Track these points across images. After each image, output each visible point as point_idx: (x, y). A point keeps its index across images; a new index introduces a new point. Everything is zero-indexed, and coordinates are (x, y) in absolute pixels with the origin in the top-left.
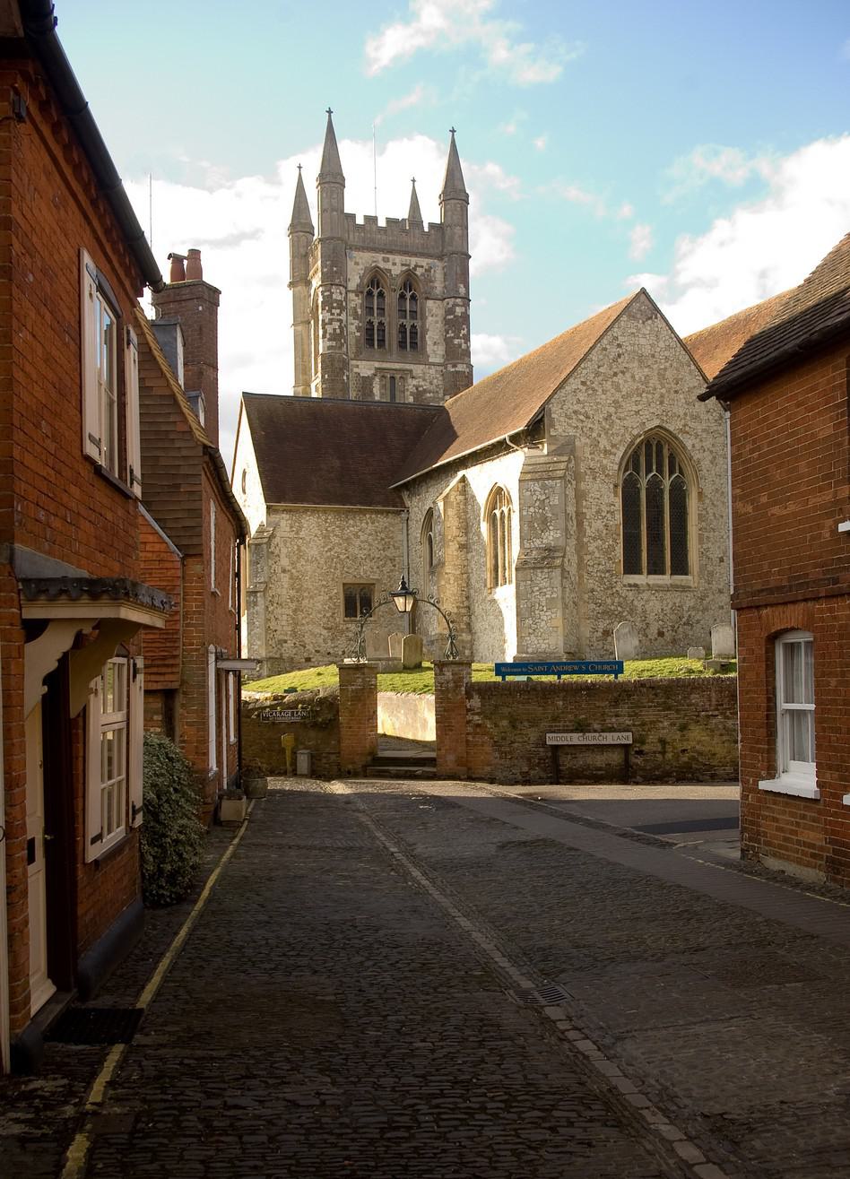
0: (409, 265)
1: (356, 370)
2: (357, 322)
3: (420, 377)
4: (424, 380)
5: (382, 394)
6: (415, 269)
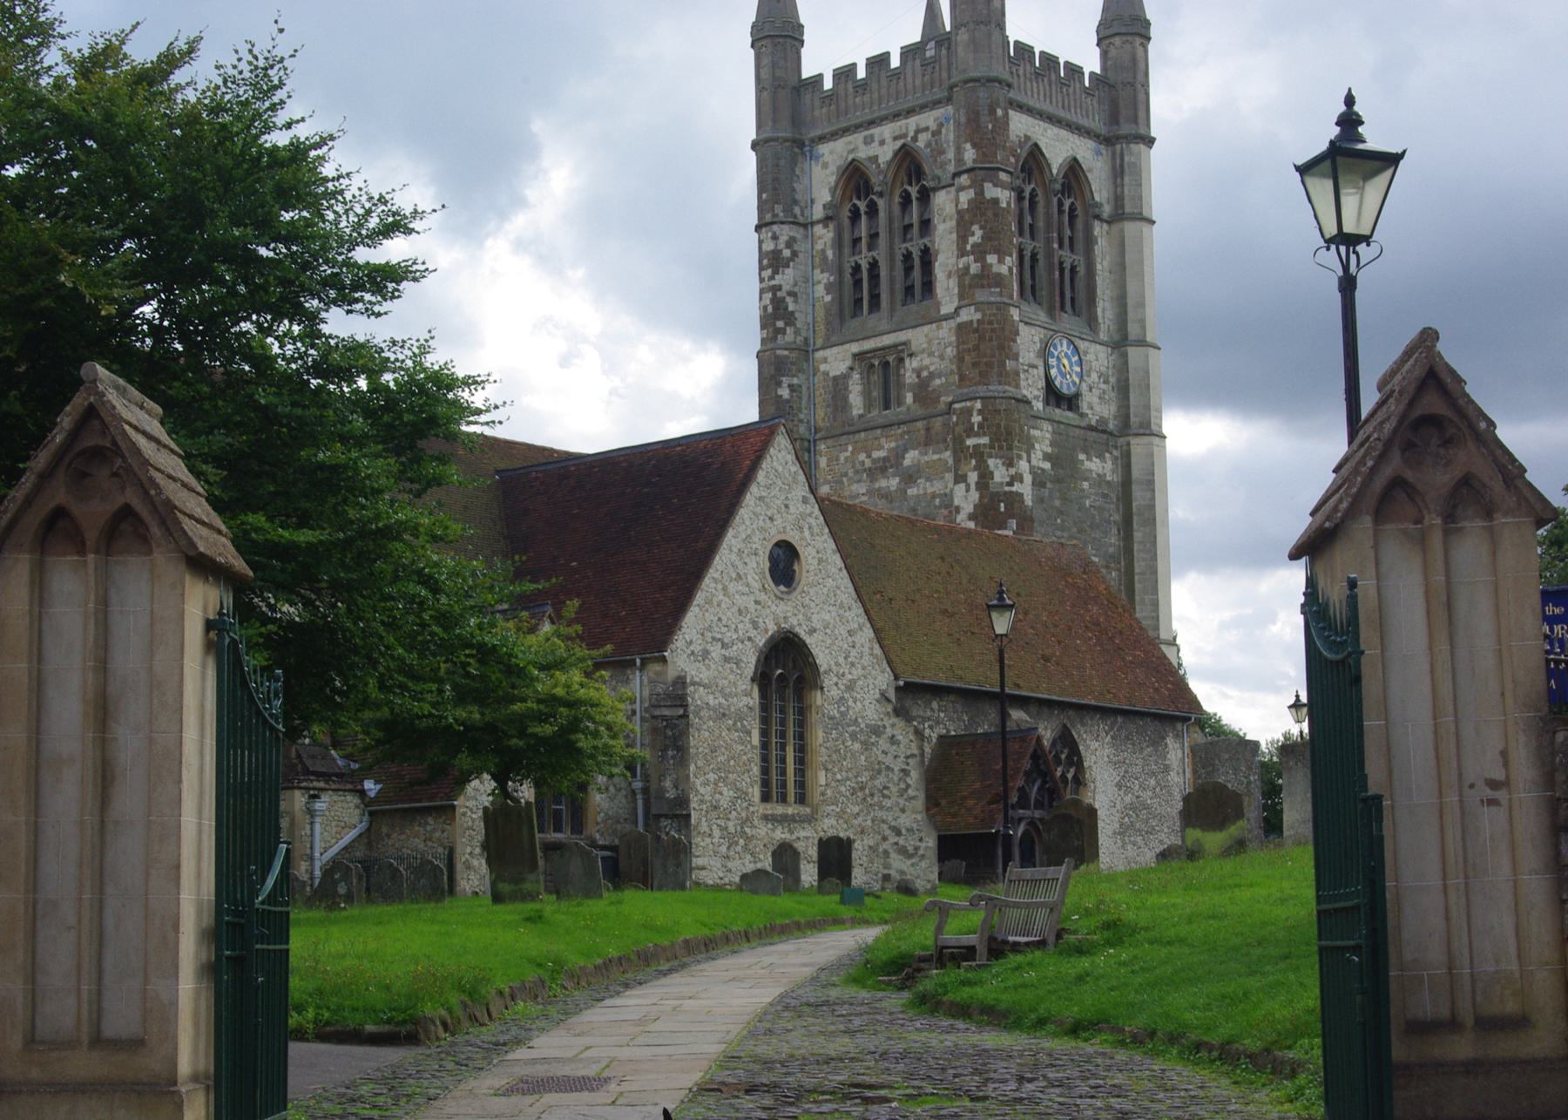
0: (905, 136)
1: (823, 367)
2: (826, 275)
3: (923, 351)
4: (931, 354)
5: (869, 406)
6: (915, 139)
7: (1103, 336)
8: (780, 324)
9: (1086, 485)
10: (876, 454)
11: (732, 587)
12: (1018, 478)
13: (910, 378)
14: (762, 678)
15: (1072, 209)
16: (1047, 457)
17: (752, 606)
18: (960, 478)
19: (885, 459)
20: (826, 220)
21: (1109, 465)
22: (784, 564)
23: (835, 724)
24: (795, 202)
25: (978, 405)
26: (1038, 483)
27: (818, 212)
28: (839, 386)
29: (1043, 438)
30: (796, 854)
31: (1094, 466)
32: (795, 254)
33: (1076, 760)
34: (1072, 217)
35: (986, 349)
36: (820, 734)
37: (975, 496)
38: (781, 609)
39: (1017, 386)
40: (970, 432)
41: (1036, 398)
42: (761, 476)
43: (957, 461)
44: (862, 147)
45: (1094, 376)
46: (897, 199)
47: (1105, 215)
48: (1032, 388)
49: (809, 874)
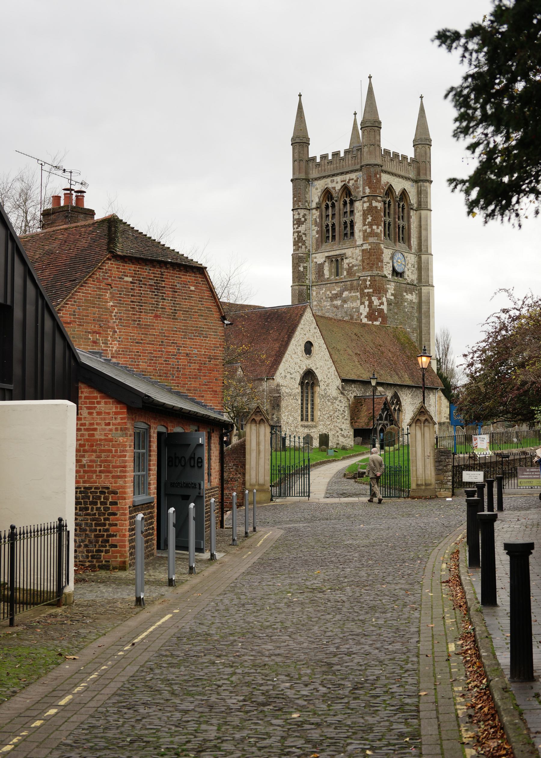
0: (345, 181)
1: (315, 260)
4: (353, 258)
5: (331, 274)
6: (349, 182)
7: (413, 251)
8: (300, 244)
9: (406, 304)
10: (333, 292)
11: (293, 356)
12: (382, 303)
13: (345, 266)
14: (302, 384)
15: (403, 206)
16: (392, 295)
17: (299, 361)
18: (362, 303)
19: (336, 294)
20: (317, 208)
21: (414, 296)
22: (308, 348)
23: (323, 396)
24: (306, 201)
25: (369, 278)
26: (389, 304)
27: (314, 205)
28: (320, 268)
29: (391, 288)
30: (312, 438)
31: (409, 297)
32: (306, 220)
33: (399, 403)
34: (403, 209)
35: (372, 258)
36: (319, 400)
37: (367, 309)
38: (307, 362)
39: (383, 271)
40: (366, 287)
41: (389, 274)
42: (302, 321)
43: (361, 297)
44: (330, 183)
45: (410, 265)
46: (342, 203)
47: (415, 208)
48: (387, 271)
49: (316, 443)
